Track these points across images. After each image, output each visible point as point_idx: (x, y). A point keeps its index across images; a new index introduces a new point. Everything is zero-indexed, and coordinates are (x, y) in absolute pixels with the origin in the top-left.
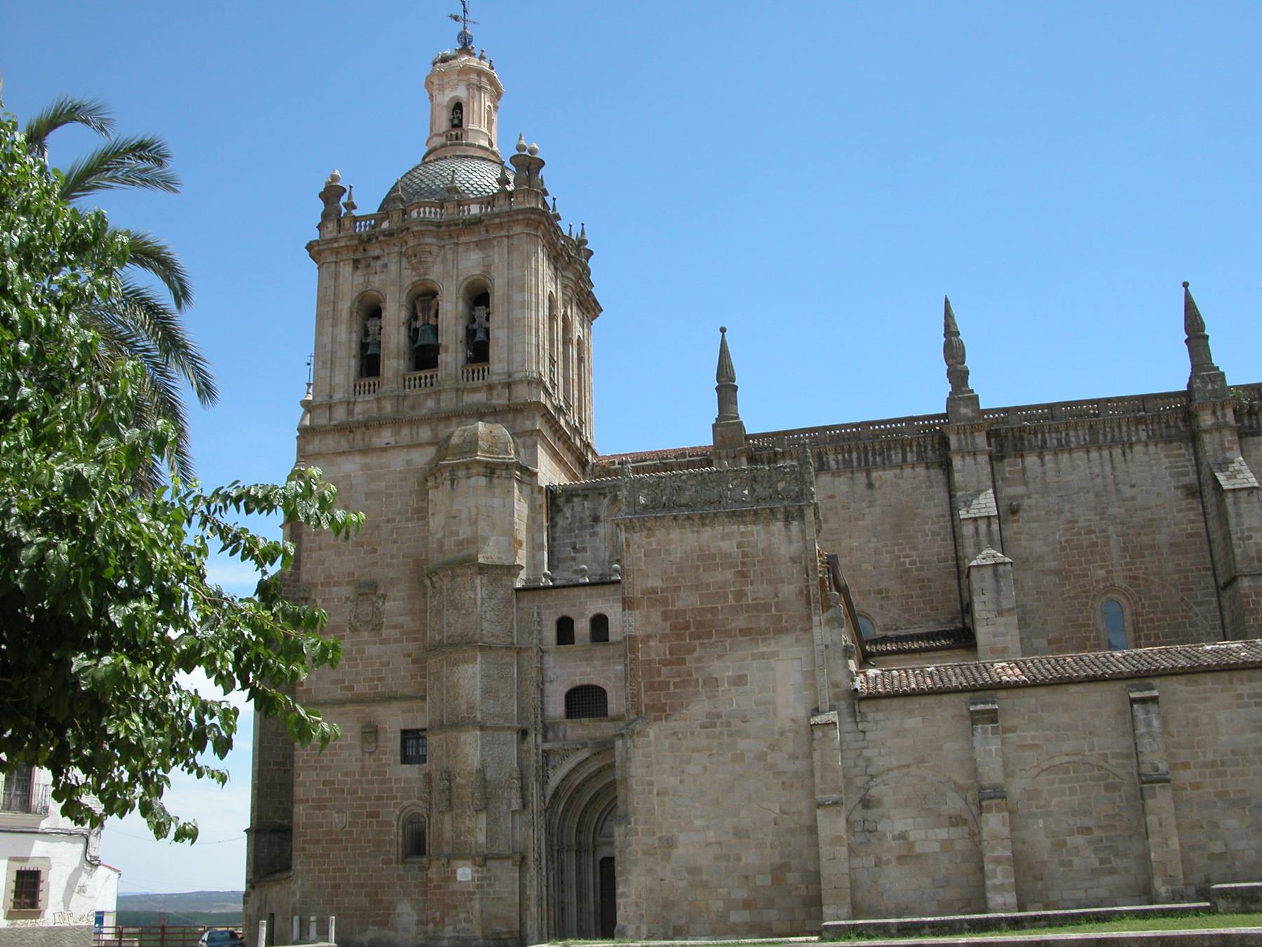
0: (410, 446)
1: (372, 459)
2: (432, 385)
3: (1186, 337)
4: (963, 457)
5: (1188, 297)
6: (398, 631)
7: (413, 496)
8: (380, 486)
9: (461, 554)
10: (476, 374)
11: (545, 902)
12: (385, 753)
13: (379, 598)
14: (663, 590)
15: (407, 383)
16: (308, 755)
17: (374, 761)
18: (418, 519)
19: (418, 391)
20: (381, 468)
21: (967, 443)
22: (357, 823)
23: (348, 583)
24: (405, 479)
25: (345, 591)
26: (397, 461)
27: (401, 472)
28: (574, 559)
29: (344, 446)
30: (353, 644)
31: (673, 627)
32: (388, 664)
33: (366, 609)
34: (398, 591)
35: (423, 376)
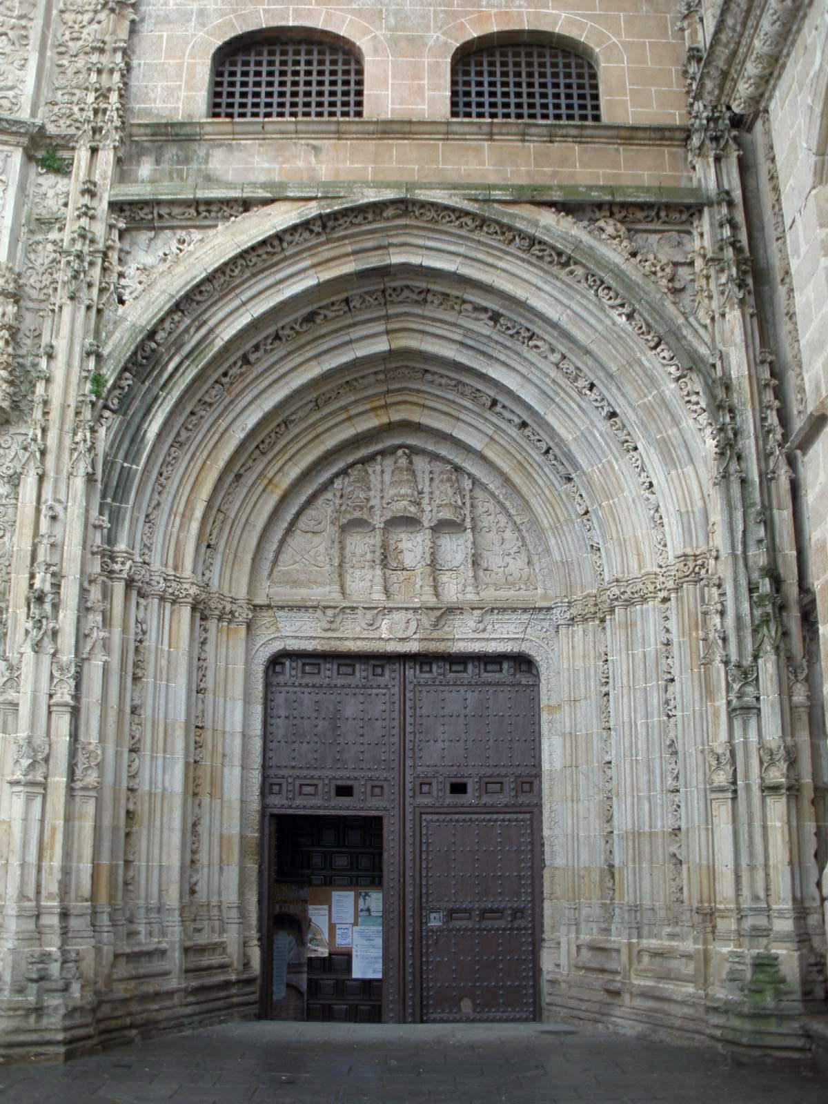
11: (59, 780)
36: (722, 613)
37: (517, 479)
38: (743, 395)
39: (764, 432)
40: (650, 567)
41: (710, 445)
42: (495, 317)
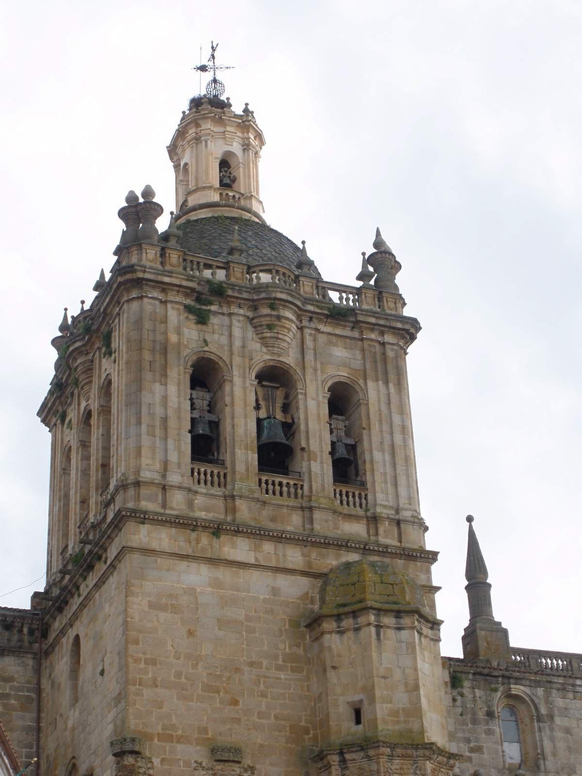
0: (277, 570)
1: (224, 574)
2: (296, 496)
7: (283, 637)
8: (239, 614)
9: (397, 728)
10: (351, 499)
13: (246, 770)
15: (264, 485)
18: (293, 670)
19: (278, 500)
20: (238, 590)
24: (272, 611)
25: (195, 753)
29: (187, 550)
34: (272, 764)
35: (285, 481)
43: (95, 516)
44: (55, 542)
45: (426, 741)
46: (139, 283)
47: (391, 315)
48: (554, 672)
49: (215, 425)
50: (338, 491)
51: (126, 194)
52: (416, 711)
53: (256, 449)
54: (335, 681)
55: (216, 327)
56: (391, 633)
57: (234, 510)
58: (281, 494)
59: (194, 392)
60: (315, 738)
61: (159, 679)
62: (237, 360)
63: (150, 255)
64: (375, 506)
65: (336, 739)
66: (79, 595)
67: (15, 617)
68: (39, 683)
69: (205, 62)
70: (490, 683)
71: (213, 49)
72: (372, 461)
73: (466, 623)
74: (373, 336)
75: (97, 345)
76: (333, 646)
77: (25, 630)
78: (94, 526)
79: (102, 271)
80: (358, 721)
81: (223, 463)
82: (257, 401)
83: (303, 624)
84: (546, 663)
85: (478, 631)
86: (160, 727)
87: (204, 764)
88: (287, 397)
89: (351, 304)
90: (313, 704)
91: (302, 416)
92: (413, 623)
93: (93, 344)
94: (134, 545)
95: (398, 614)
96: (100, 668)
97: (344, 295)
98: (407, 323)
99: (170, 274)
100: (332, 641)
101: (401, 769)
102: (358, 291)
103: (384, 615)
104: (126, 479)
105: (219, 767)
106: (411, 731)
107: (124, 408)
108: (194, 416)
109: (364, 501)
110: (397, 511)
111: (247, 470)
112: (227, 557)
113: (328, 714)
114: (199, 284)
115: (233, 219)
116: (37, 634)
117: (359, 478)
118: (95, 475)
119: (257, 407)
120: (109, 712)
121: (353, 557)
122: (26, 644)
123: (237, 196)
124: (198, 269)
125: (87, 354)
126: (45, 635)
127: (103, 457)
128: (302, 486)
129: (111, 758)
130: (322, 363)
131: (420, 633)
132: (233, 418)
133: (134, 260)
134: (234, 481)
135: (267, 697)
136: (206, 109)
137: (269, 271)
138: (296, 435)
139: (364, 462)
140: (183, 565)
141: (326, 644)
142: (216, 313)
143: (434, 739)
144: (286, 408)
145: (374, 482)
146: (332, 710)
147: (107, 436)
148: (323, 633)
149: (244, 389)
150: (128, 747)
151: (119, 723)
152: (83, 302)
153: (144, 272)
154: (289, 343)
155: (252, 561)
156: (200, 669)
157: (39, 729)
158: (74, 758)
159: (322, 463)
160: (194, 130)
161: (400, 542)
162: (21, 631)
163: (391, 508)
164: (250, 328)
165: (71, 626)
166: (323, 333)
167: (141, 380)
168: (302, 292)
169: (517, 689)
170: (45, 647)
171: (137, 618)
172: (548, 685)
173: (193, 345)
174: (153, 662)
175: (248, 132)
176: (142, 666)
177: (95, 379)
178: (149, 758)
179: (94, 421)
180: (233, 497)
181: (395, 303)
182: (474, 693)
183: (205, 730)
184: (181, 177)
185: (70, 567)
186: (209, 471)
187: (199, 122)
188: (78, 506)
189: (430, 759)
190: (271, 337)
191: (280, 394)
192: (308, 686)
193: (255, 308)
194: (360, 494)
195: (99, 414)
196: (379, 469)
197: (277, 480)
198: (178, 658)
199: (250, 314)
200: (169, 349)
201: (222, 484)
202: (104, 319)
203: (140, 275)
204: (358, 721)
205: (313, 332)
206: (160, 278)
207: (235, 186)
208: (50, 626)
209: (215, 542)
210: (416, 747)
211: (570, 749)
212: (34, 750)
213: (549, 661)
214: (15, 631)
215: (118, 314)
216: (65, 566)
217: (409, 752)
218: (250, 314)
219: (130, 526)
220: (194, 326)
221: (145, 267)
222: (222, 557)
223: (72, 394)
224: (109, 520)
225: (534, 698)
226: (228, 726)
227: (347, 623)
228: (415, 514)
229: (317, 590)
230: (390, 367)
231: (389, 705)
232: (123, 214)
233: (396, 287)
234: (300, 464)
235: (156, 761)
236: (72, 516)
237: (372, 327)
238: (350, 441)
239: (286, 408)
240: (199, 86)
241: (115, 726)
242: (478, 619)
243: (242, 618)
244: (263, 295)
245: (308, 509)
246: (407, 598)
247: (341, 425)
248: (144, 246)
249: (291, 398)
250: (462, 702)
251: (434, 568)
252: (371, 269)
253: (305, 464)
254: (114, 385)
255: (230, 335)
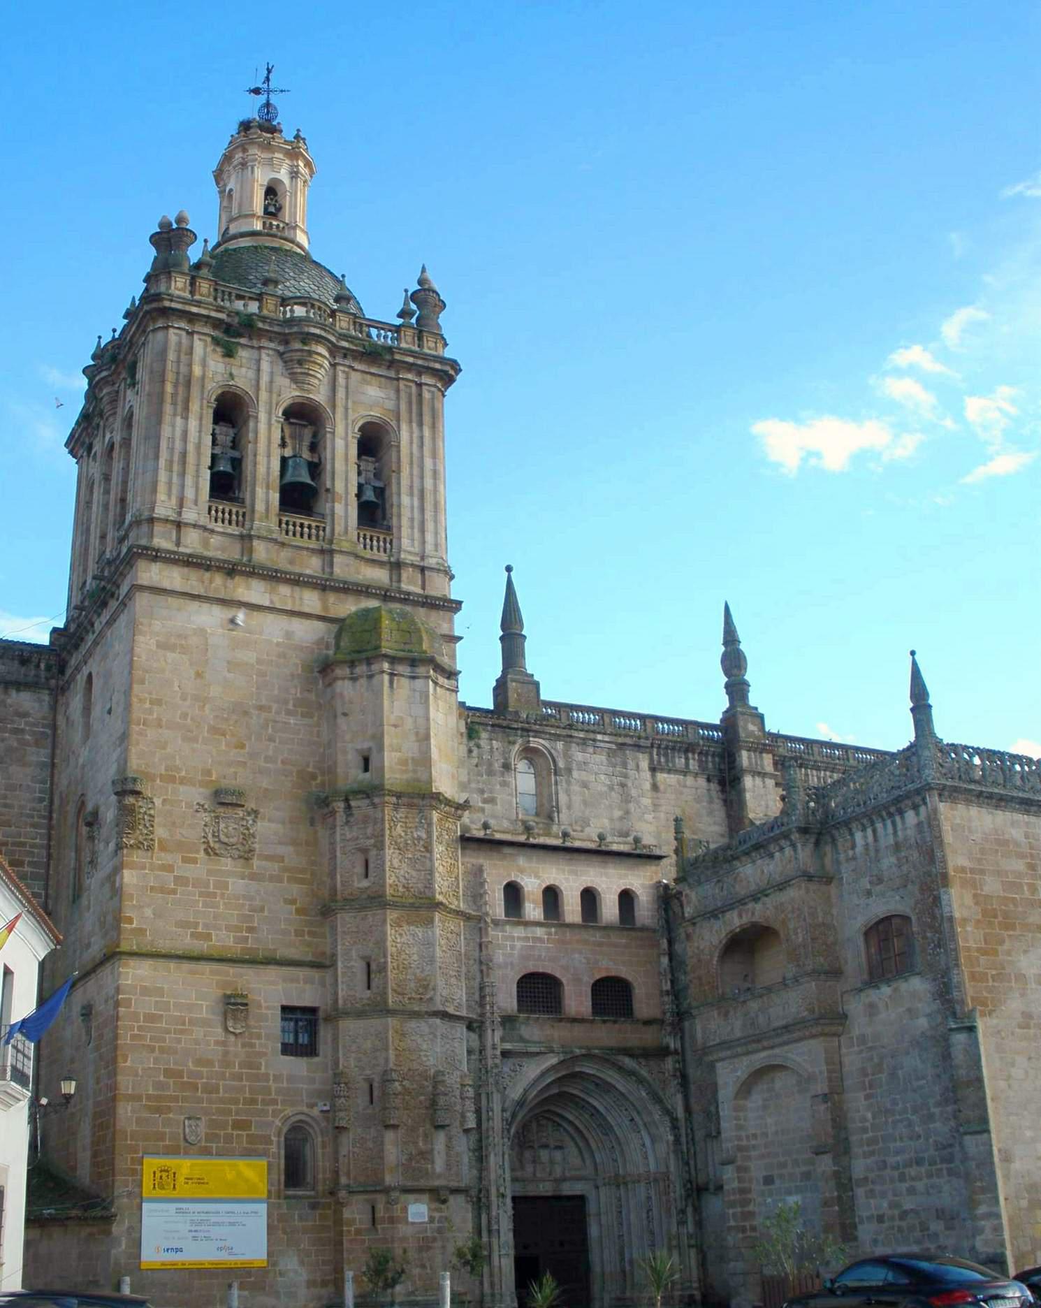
3: (911, 705)
4: (753, 776)
5: (914, 664)
6: (276, 866)
9: (405, 777)
10: (375, 543)
12: (259, 1037)
13: (249, 814)
14: (972, 871)
15: (284, 526)
16: (140, 1028)
17: (244, 1045)
18: (303, 715)
19: (298, 541)
21: (756, 764)
22: (217, 1136)
23: (203, 784)
25: (196, 794)
26: (274, 629)
27: (278, 644)
28: (483, 810)
29: (199, 590)
30: (210, 872)
31: (985, 913)
32: (262, 909)
33: (229, 828)
35: (306, 523)
36: (675, 1192)
37: (585, 1132)
38: (682, 1123)
39: (687, 1135)
40: (641, 1171)
41: (671, 1138)
42: (597, 1085)
43: (111, 551)
44: (75, 577)
45: (434, 790)
46: (166, 312)
47: (430, 355)
48: (586, 727)
49: (237, 463)
50: (362, 535)
51: (159, 219)
52: (425, 760)
53: (278, 489)
54: (345, 728)
55: (244, 361)
56: (405, 681)
57: (251, 551)
58: (302, 535)
59: (217, 427)
60: (323, 784)
61: (164, 720)
62: (264, 395)
63: (179, 286)
64: (399, 552)
65: (343, 784)
66: (93, 633)
67: (31, 653)
68: (54, 719)
69: (260, 85)
70: (508, 736)
71: (269, 71)
72: (399, 506)
73: (499, 674)
74: (410, 376)
75: (123, 375)
76: (345, 693)
77: (42, 666)
78: (109, 563)
79: (134, 298)
80: (366, 769)
81: (242, 502)
82: (283, 438)
83: (316, 670)
84: (578, 717)
85: (509, 683)
86: (163, 767)
87: (206, 806)
88: (315, 435)
89: (389, 342)
90: (322, 750)
91: (329, 456)
92: (428, 672)
93: (119, 374)
94: (145, 583)
95: (413, 663)
96: (108, 707)
97: (382, 332)
98: (446, 364)
99: (198, 304)
100: (345, 688)
101: (406, 817)
102: (397, 329)
103: (399, 663)
104: (141, 515)
105: (221, 810)
106: (418, 780)
107: (142, 441)
108: (215, 452)
109: (388, 545)
110: (423, 558)
111: (267, 510)
112: (241, 599)
113: (335, 763)
114: (228, 315)
115: (272, 249)
116: (55, 670)
117: (385, 523)
118: (113, 510)
119: (283, 445)
120: (114, 751)
121: (373, 603)
122: (43, 680)
123: (281, 225)
124: (230, 300)
125: (114, 384)
126: (62, 671)
127: (122, 491)
128: (324, 528)
129: (114, 798)
130: (354, 402)
131: (436, 683)
132: (255, 455)
133: (163, 288)
134: (252, 520)
135: (275, 741)
136: (255, 133)
137: (304, 304)
138: (323, 474)
139: (392, 505)
140: (194, 605)
141: (338, 690)
142: (243, 346)
143: (441, 790)
144: (313, 447)
145: (400, 527)
146: (340, 758)
147: (126, 470)
148: (336, 679)
149: (270, 425)
150: (130, 786)
151: (122, 762)
152: (114, 331)
153: (171, 301)
154: (320, 380)
155: (267, 603)
156: (207, 711)
157: (53, 765)
158: (82, 795)
159: (347, 505)
160: (241, 155)
161: (423, 588)
162: (38, 666)
163: (416, 554)
164: (281, 363)
165: (86, 663)
166: (357, 370)
167: (161, 412)
168: (337, 328)
169: (535, 742)
170: (61, 683)
171: (144, 657)
172: (569, 739)
173: (219, 378)
174: (158, 702)
175: (297, 160)
176: (147, 705)
177: (119, 410)
178: (151, 799)
179: (115, 454)
180: (250, 537)
181: (436, 343)
182: (491, 744)
183: (209, 773)
184: (225, 204)
185: (86, 603)
186: (227, 510)
187: (247, 146)
188: (97, 541)
189: (436, 808)
190: (302, 373)
191: (307, 433)
192: (318, 731)
193: (287, 343)
194: (385, 539)
195: (121, 447)
196: (406, 514)
197: (298, 521)
198: (185, 700)
199: (281, 348)
200: (193, 382)
201: (240, 524)
202: (130, 348)
203: (167, 304)
204: (366, 769)
205: (346, 369)
206: (187, 308)
207: (280, 214)
208: (67, 662)
209: (230, 583)
210: (423, 797)
211: (585, 803)
212: (48, 785)
213: (580, 715)
214: (32, 667)
215: (143, 344)
216: (82, 602)
217: (415, 801)
218: (281, 348)
219: (142, 565)
220: (221, 359)
221: (173, 296)
222: (236, 599)
223: (98, 425)
224: (122, 555)
225: (553, 751)
226: (232, 770)
227: (361, 669)
228: (440, 561)
229: (333, 636)
230: (426, 409)
231: (398, 754)
232: (156, 240)
233: (439, 326)
234: (323, 506)
235: (158, 801)
236: (91, 550)
237: (410, 367)
238: (379, 484)
239: (313, 447)
240: (251, 109)
241: (119, 765)
242: (510, 670)
243: (253, 661)
244: (295, 329)
245: (327, 553)
246: (425, 647)
247: (371, 467)
248: (173, 274)
249: (320, 436)
250: (479, 753)
251: (458, 617)
252: (413, 306)
253: (328, 505)
254: (135, 418)
255: (258, 370)
